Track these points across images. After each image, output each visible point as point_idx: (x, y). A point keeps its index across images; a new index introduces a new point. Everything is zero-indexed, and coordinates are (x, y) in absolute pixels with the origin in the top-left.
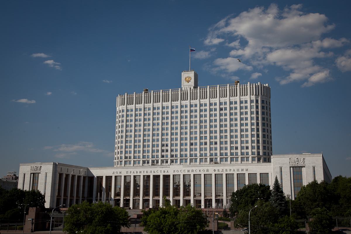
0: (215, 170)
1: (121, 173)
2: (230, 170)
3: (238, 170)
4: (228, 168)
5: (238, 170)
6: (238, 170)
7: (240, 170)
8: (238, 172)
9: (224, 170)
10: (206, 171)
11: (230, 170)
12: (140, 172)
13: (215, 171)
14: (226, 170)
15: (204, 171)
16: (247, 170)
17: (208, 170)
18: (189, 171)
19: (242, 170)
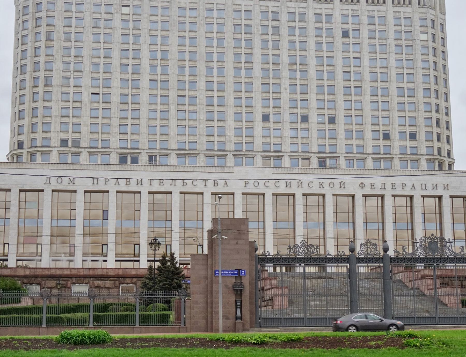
0: (362, 186)
1: (72, 180)
2: (404, 186)
3: (424, 187)
4: (398, 181)
5: (424, 187)
6: (424, 187)
7: (429, 186)
8: (425, 193)
9: (388, 186)
10: (337, 186)
11: (404, 186)
12: (140, 181)
13: (362, 187)
14: (393, 186)
15: (332, 186)
16: (446, 187)
17: (342, 185)
18: (288, 185)
19: (435, 187)
